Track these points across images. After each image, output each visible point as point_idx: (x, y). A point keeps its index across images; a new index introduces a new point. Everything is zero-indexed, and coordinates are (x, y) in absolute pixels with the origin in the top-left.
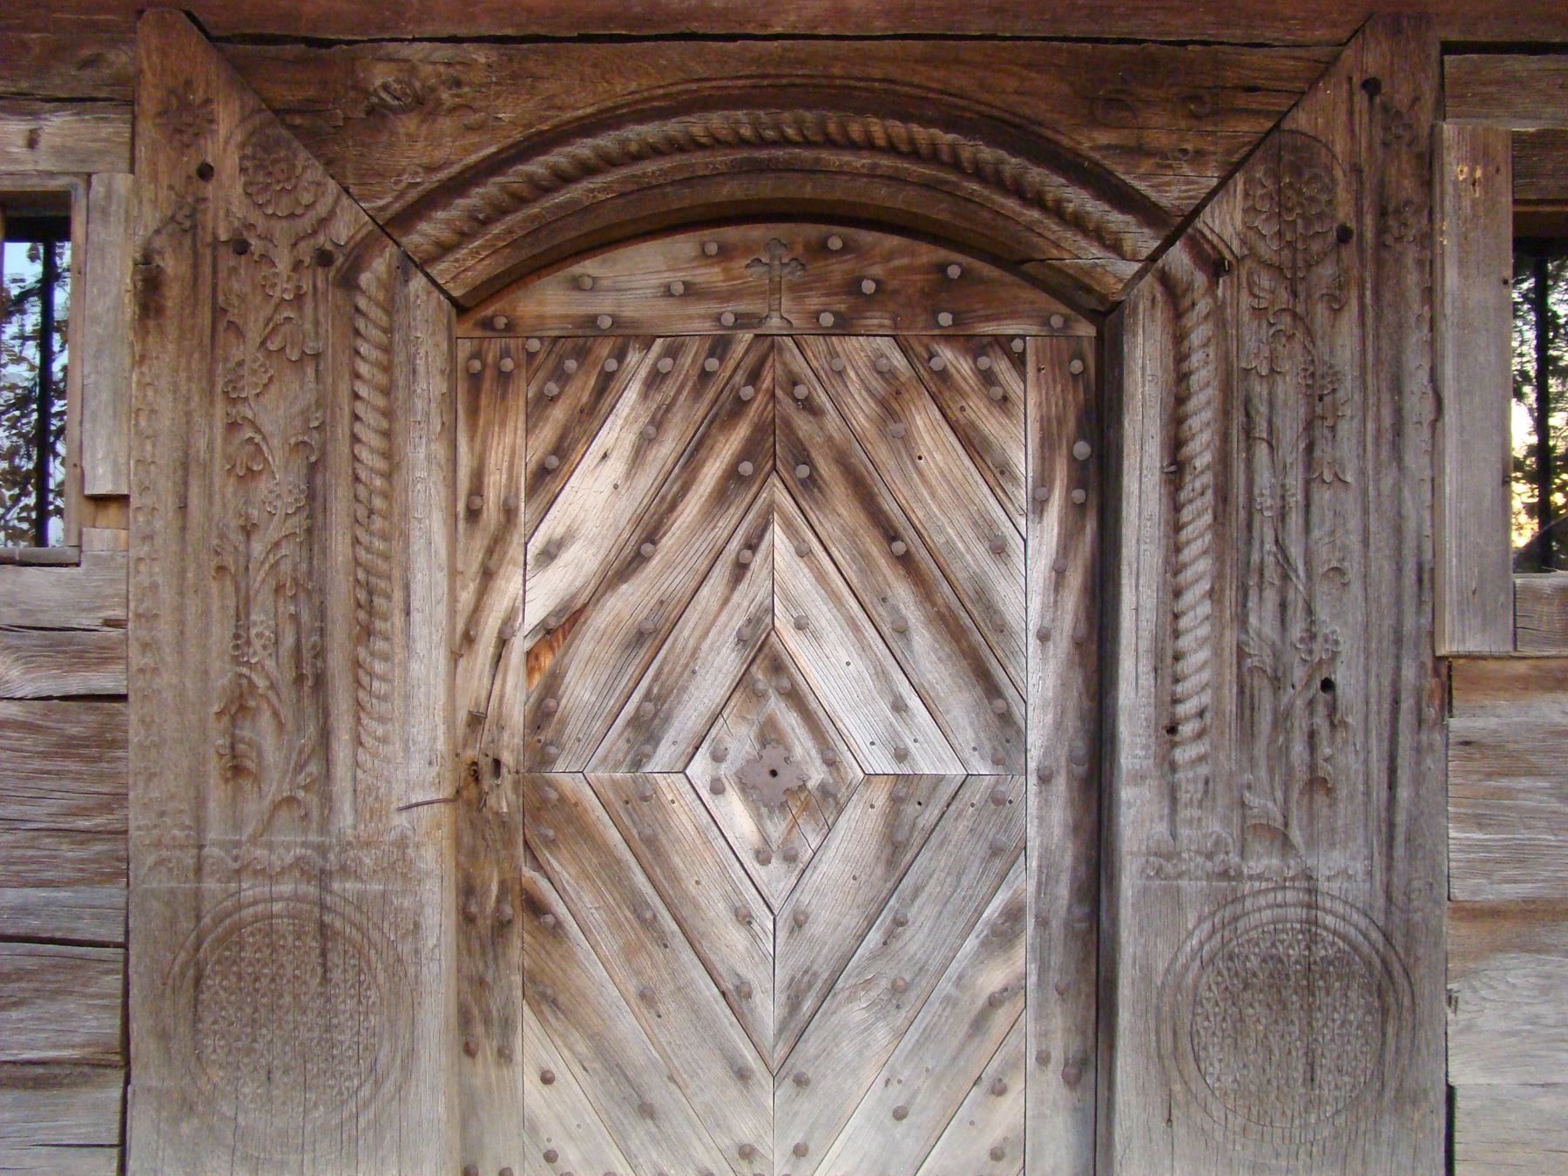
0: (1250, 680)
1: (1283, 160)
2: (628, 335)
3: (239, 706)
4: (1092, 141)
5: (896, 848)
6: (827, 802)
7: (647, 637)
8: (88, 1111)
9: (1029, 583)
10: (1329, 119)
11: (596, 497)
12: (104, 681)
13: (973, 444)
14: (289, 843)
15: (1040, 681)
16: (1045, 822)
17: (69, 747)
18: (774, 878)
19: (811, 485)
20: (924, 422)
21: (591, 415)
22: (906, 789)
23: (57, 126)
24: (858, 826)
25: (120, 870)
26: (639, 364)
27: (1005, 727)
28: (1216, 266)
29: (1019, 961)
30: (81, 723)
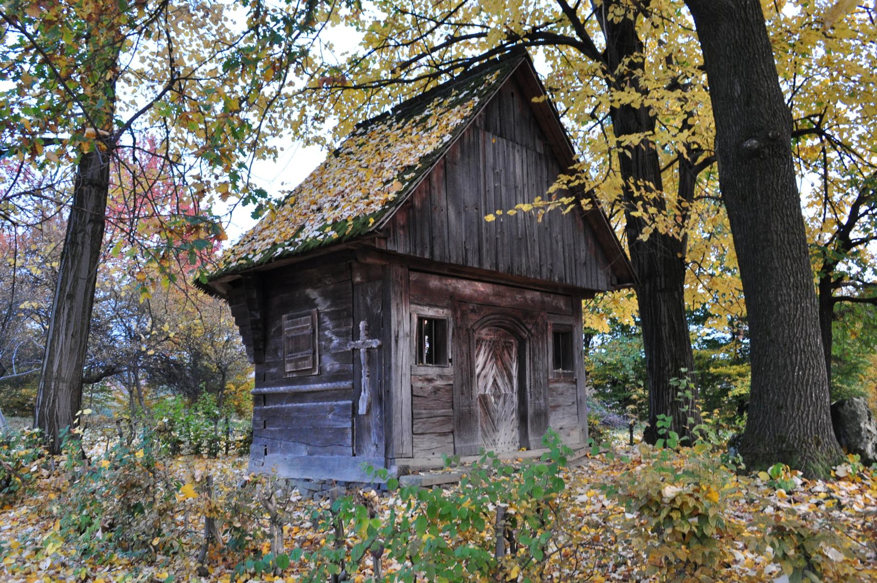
0: (536, 381)
1: (536, 324)
2: (483, 340)
3: (462, 386)
4: (524, 321)
5: (505, 402)
6: (499, 397)
7: (485, 377)
8: (450, 438)
9: (514, 372)
10: (539, 320)
11: (480, 360)
12: (451, 382)
13: (510, 355)
14: (467, 403)
15: (515, 381)
16: (515, 399)
17: (447, 391)
18: (495, 406)
19: (497, 359)
20: (505, 352)
21: (480, 349)
22: (506, 395)
23: (445, 311)
24: (502, 399)
25: (452, 407)
26: (484, 343)
27: (512, 388)
28: (532, 335)
29: (514, 416)
30: (448, 388)
